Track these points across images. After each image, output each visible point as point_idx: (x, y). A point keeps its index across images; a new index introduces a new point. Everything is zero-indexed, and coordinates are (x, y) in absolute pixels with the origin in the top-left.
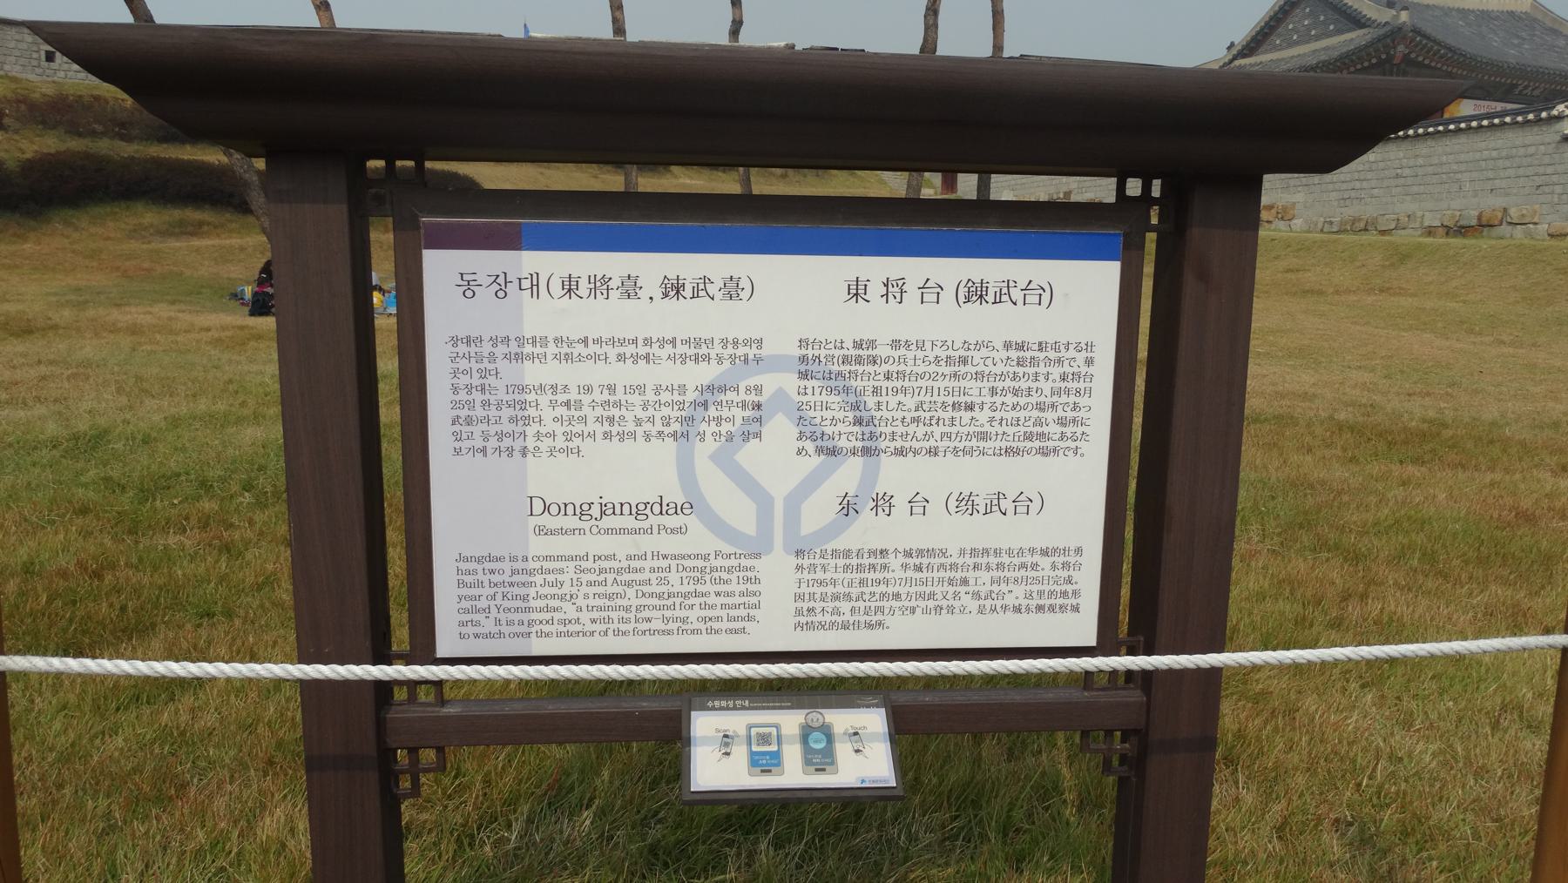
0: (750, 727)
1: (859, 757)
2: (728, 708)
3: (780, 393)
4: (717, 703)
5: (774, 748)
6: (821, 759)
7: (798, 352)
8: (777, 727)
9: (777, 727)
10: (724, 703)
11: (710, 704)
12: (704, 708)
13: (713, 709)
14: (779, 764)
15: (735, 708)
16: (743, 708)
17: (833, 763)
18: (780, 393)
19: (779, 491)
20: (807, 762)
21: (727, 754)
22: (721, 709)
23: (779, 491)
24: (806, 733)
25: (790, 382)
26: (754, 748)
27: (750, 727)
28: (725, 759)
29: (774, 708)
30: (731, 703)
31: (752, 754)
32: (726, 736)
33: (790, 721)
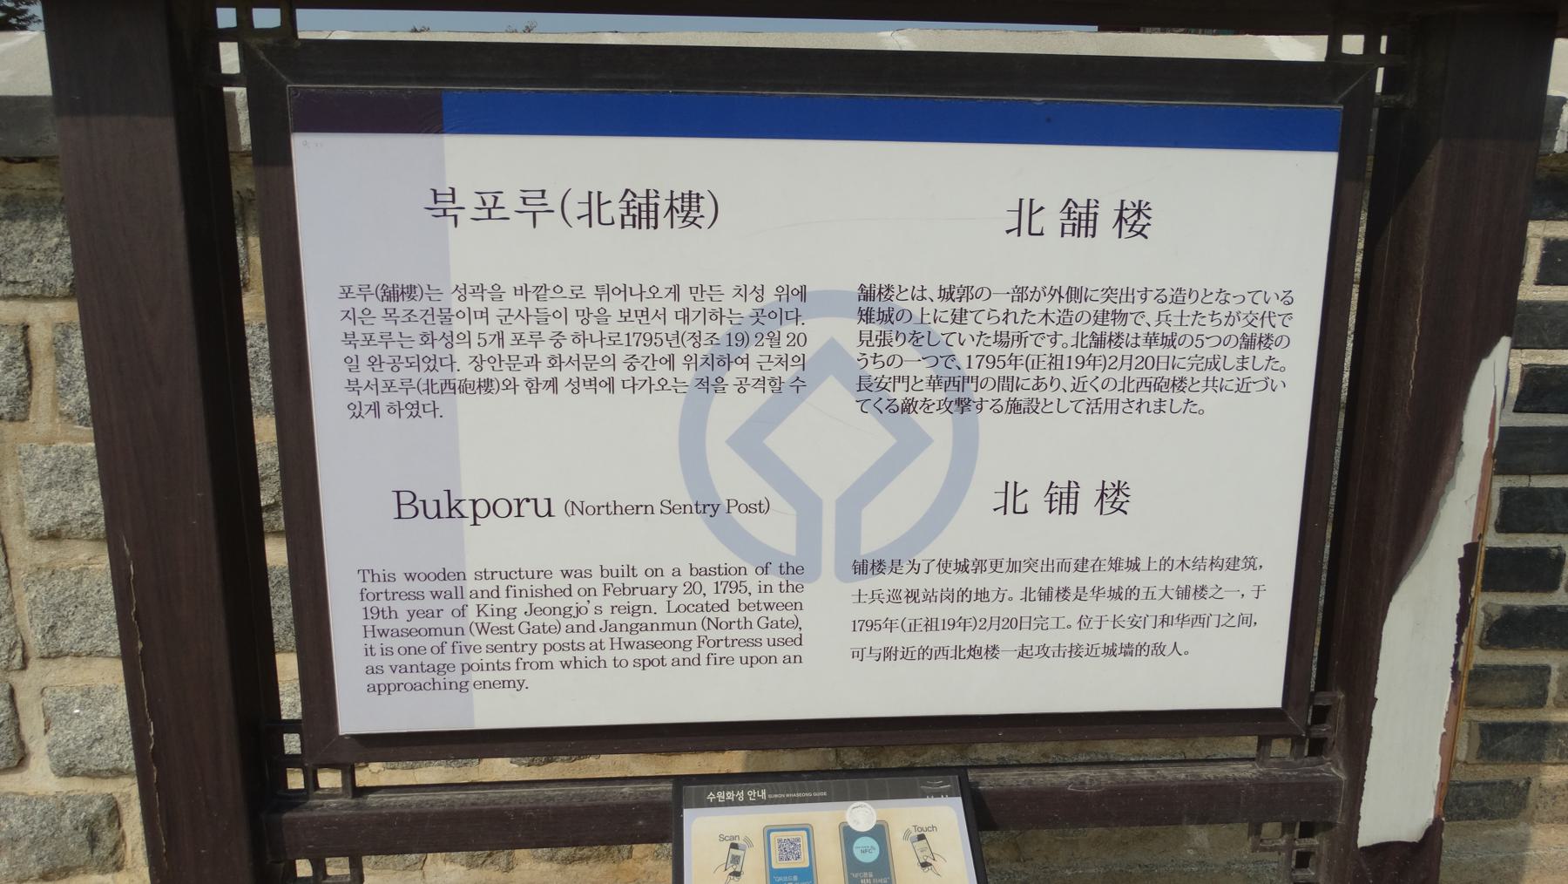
0: (768, 831)
1: (929, 873)
2: (736, 803)
3: (832, 346)
4: (721, 796)
5: (803, 863)
8: (808, 829)
9: (808, 829)
10: (730, 795)
12: (702, 803)
13: (716, 804)
15: (747, 802)
16: (759, 802)
18: (832, 346)
21: (736, 874)
22: (728, 803)
25: (846, 330)
26: (777, 865)
29: (802, 800)
30: (740, 794)
32: (734, 846)
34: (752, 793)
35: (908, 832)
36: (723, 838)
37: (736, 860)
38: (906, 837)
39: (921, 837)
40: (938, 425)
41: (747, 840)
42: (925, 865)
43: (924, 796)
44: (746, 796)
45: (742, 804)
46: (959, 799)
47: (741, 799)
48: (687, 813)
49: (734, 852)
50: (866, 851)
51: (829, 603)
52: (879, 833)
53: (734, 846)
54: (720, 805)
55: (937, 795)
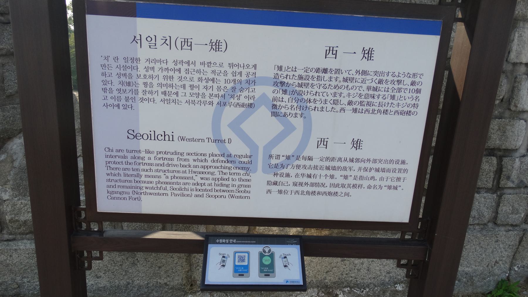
0: (235, 253)
4: (221, 241)
5: (247, 264)
6: (267, 269)
7: (276, 71)
8: (248, 253)
10: (224, 241)
11: (218, 241)
12: (215, 243)
13: (219, 243)
14: (248, 272)
15: (229, 243)
16: (233, 243)
17: (273, 272)
19: (261, 144)
20: (261, 271)
21: (224, 266)
22: (223, 243)
23: (261, 144)
24: (261, 256)
26: (237, 264)
27: (235, 253)
28: (222, 268)
31: (235, 266)
32: (224, 257)
33: (254, 251)
34: (231, 240)
35: (281, 255)
36: (220, 254)
37: (224, 261)
38: (280, 257)
39: (285, 257)
40: (298, 122)
41: (228, 255)
42: (285, 266)
43: (287, 244)
44: (229, 241)
45: (227, 244)
46: (299, 246)
47: (227, 242)
48: (210, 246)
49: (224, 259)
50: (267, 261)
51: (259, 178)
52: (272, 256)
53: (224, 257)
54: (220, 244)
55: (292, 244)
